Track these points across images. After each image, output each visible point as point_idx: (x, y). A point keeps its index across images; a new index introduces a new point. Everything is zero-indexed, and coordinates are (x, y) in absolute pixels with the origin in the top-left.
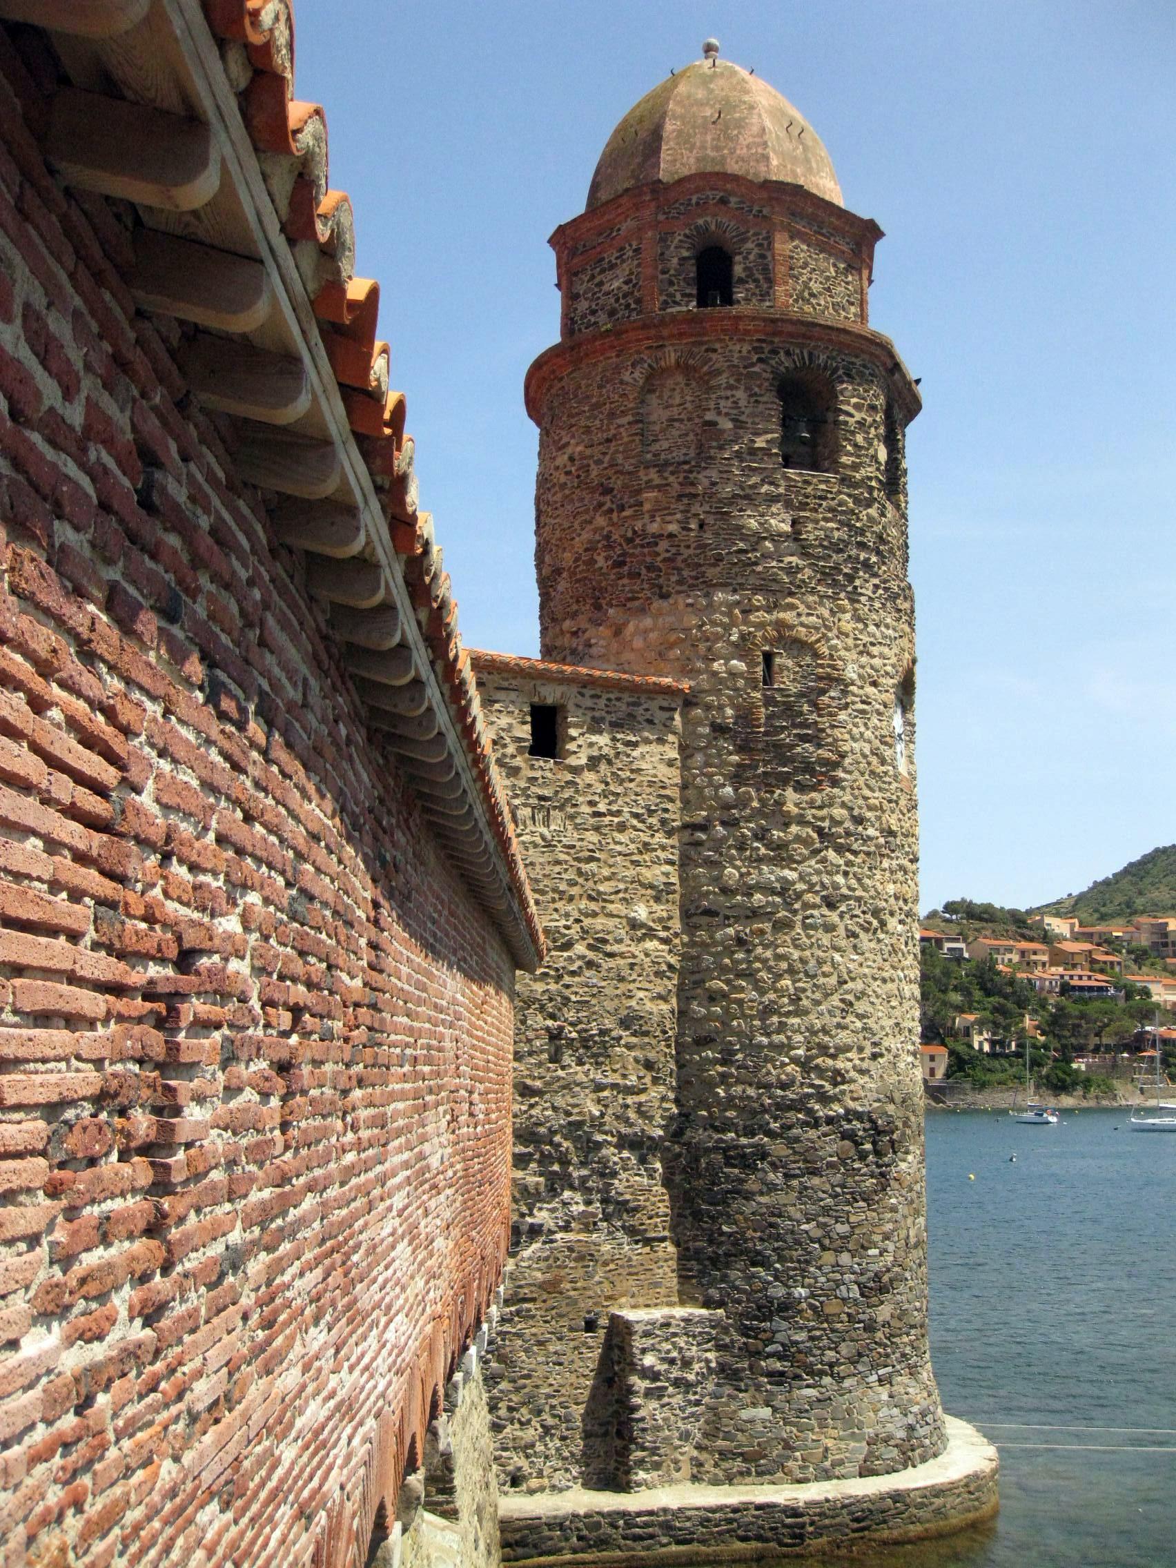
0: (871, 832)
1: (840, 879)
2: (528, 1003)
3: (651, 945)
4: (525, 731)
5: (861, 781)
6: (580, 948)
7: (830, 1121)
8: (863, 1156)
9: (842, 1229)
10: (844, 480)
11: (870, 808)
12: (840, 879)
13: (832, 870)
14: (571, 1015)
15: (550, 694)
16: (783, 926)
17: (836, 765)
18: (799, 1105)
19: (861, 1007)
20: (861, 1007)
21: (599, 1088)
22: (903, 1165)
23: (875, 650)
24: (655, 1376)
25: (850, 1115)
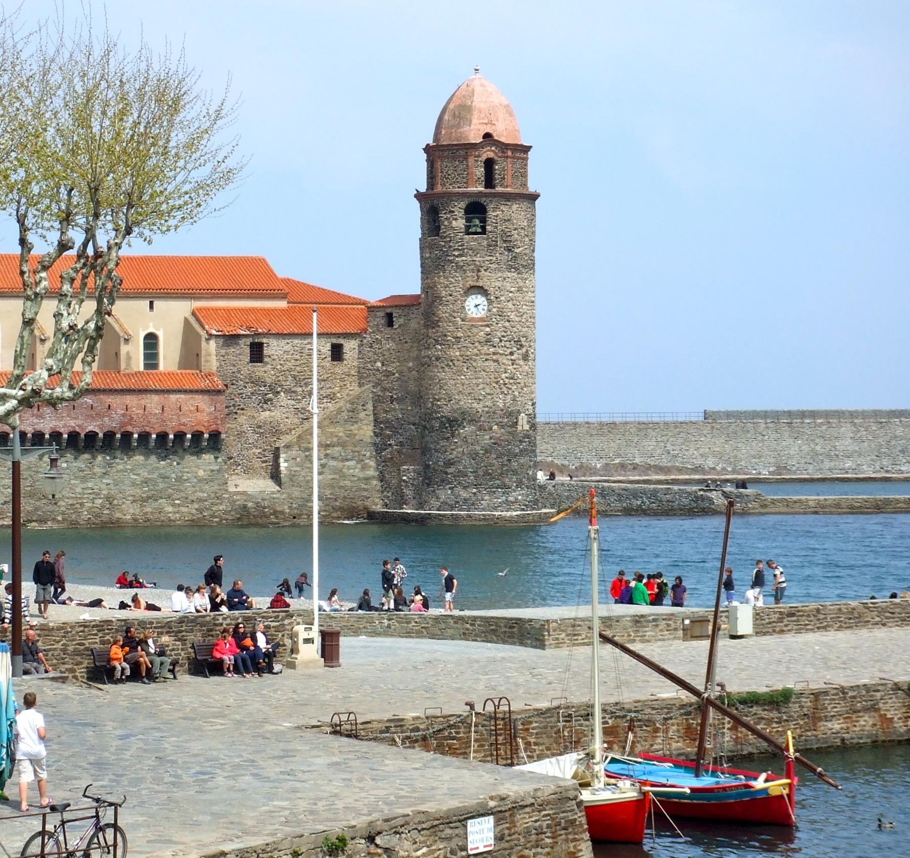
0: (449, 338)
1: (439, 353)
2: (385, 389)
3: (414, 372)
4: (382, 322)
5: (445, 325)
6: (397, 375)
7: (438, 418)
8: (446, 428)
9: (438, 447)
10: (441, 237)
11: (449, 332)
12: (439, 353)
13: (437, 350)
14: (395, 392)
15: (389, 311)
16: (429, 366)
17: (438, 321)
18: (431, 414)
19: (445, 387)
20: (445, 387)
21: (402, 409)
22: (462, 431)
23: (451, 286)
24: (407, 482)
25: (442, 417)
